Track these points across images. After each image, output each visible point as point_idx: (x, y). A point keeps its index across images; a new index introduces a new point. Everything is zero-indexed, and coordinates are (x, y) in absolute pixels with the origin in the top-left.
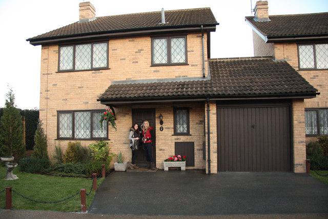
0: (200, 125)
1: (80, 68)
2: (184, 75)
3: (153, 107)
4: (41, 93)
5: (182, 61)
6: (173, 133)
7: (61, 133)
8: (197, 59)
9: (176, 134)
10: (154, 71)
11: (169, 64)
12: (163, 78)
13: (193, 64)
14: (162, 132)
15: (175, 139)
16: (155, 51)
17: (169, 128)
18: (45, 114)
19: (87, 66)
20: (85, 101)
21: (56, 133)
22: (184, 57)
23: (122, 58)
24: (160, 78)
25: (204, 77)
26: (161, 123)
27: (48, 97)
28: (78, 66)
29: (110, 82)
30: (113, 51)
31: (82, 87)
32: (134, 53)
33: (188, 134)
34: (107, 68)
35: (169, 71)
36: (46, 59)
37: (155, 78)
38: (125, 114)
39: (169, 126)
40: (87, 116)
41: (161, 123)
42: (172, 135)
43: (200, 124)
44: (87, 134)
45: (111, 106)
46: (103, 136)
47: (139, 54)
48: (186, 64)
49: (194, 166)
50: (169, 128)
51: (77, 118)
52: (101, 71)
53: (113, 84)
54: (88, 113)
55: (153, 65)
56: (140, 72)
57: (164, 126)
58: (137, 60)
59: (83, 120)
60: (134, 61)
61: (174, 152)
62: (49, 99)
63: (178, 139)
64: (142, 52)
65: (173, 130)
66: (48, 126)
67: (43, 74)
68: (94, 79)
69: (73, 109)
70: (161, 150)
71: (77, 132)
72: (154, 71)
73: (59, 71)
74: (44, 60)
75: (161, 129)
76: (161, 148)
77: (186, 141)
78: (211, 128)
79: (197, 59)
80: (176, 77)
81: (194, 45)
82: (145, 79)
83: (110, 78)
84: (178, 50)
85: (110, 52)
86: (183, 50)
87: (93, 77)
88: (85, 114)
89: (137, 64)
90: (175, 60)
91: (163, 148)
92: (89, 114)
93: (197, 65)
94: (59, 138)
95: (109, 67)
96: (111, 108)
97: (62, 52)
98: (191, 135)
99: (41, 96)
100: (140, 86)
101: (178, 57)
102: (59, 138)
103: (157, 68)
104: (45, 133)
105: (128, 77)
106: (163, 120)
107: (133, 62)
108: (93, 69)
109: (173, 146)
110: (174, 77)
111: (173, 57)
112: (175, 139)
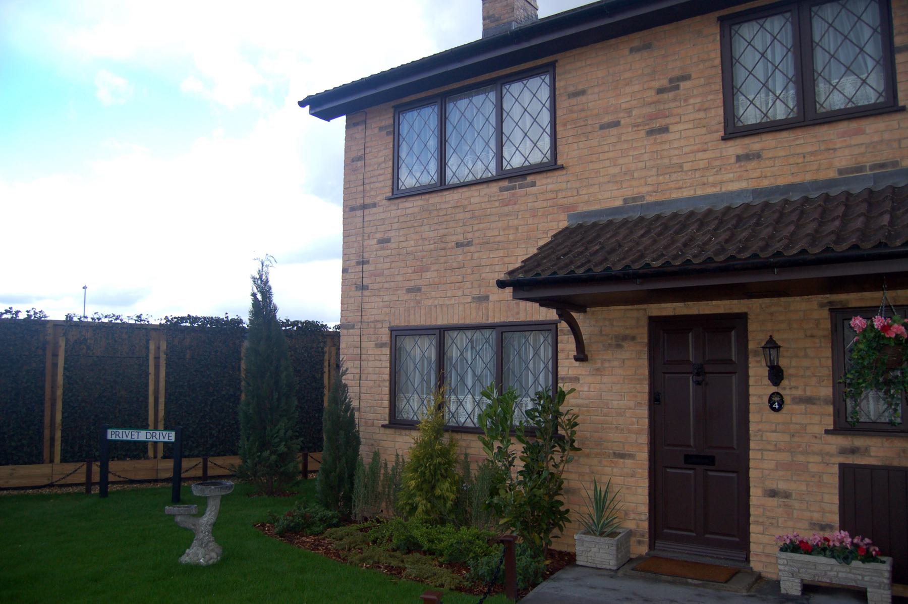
1: (464, 175)
4: (345, 271)
6: (829, 422)
10: (739, 158)
12: (781, 182)
15: (843, 451)
16: (741, 75)
17: (809, 401)
18: (357, 339)
20: (476, 292)
21: (386, 403)
23: (607, 119)
24: (765, 183)
27: (366, 282)
28: (457, 170)
30: (574, 101)
31: (469, 243)
32: (653, 93)
34: (551, 166)
36: (359, 159)
37: (743, 185)
38: (620, 341)
41: (776, 375)
42: (827, 432)
47: (671, 95)
50: (809, 401)
52: (530, 179)
57: (787, 389)
61: (836, 508)
62: (367, 288)
63: (853, 451)
64: (683, 85)
65: (830, 409)
66: (364, 382)
67: (353, 209)
69: (441, 321)
70: (773, 494)
73: (398, 194)
74: (355, 161)
75: (776, 403)
76: (772, 485)
77: (896, 463)
80: (841, 171)
82: (699, 192)
83: (561, 201)
85: (563, 104)
86: (872, 48)
87: (505, 203)
89: (665, 137)
91: (782, 486)
94: (396, 423)
96: (564, 315)
97: (404, 128)
99: (344, 279)
101: (840, 90)
103: (754, 144)
104: (355, 404)
105: (629, 193)
106: (783, 363)
107: (651, 132)
111: (822, 87)
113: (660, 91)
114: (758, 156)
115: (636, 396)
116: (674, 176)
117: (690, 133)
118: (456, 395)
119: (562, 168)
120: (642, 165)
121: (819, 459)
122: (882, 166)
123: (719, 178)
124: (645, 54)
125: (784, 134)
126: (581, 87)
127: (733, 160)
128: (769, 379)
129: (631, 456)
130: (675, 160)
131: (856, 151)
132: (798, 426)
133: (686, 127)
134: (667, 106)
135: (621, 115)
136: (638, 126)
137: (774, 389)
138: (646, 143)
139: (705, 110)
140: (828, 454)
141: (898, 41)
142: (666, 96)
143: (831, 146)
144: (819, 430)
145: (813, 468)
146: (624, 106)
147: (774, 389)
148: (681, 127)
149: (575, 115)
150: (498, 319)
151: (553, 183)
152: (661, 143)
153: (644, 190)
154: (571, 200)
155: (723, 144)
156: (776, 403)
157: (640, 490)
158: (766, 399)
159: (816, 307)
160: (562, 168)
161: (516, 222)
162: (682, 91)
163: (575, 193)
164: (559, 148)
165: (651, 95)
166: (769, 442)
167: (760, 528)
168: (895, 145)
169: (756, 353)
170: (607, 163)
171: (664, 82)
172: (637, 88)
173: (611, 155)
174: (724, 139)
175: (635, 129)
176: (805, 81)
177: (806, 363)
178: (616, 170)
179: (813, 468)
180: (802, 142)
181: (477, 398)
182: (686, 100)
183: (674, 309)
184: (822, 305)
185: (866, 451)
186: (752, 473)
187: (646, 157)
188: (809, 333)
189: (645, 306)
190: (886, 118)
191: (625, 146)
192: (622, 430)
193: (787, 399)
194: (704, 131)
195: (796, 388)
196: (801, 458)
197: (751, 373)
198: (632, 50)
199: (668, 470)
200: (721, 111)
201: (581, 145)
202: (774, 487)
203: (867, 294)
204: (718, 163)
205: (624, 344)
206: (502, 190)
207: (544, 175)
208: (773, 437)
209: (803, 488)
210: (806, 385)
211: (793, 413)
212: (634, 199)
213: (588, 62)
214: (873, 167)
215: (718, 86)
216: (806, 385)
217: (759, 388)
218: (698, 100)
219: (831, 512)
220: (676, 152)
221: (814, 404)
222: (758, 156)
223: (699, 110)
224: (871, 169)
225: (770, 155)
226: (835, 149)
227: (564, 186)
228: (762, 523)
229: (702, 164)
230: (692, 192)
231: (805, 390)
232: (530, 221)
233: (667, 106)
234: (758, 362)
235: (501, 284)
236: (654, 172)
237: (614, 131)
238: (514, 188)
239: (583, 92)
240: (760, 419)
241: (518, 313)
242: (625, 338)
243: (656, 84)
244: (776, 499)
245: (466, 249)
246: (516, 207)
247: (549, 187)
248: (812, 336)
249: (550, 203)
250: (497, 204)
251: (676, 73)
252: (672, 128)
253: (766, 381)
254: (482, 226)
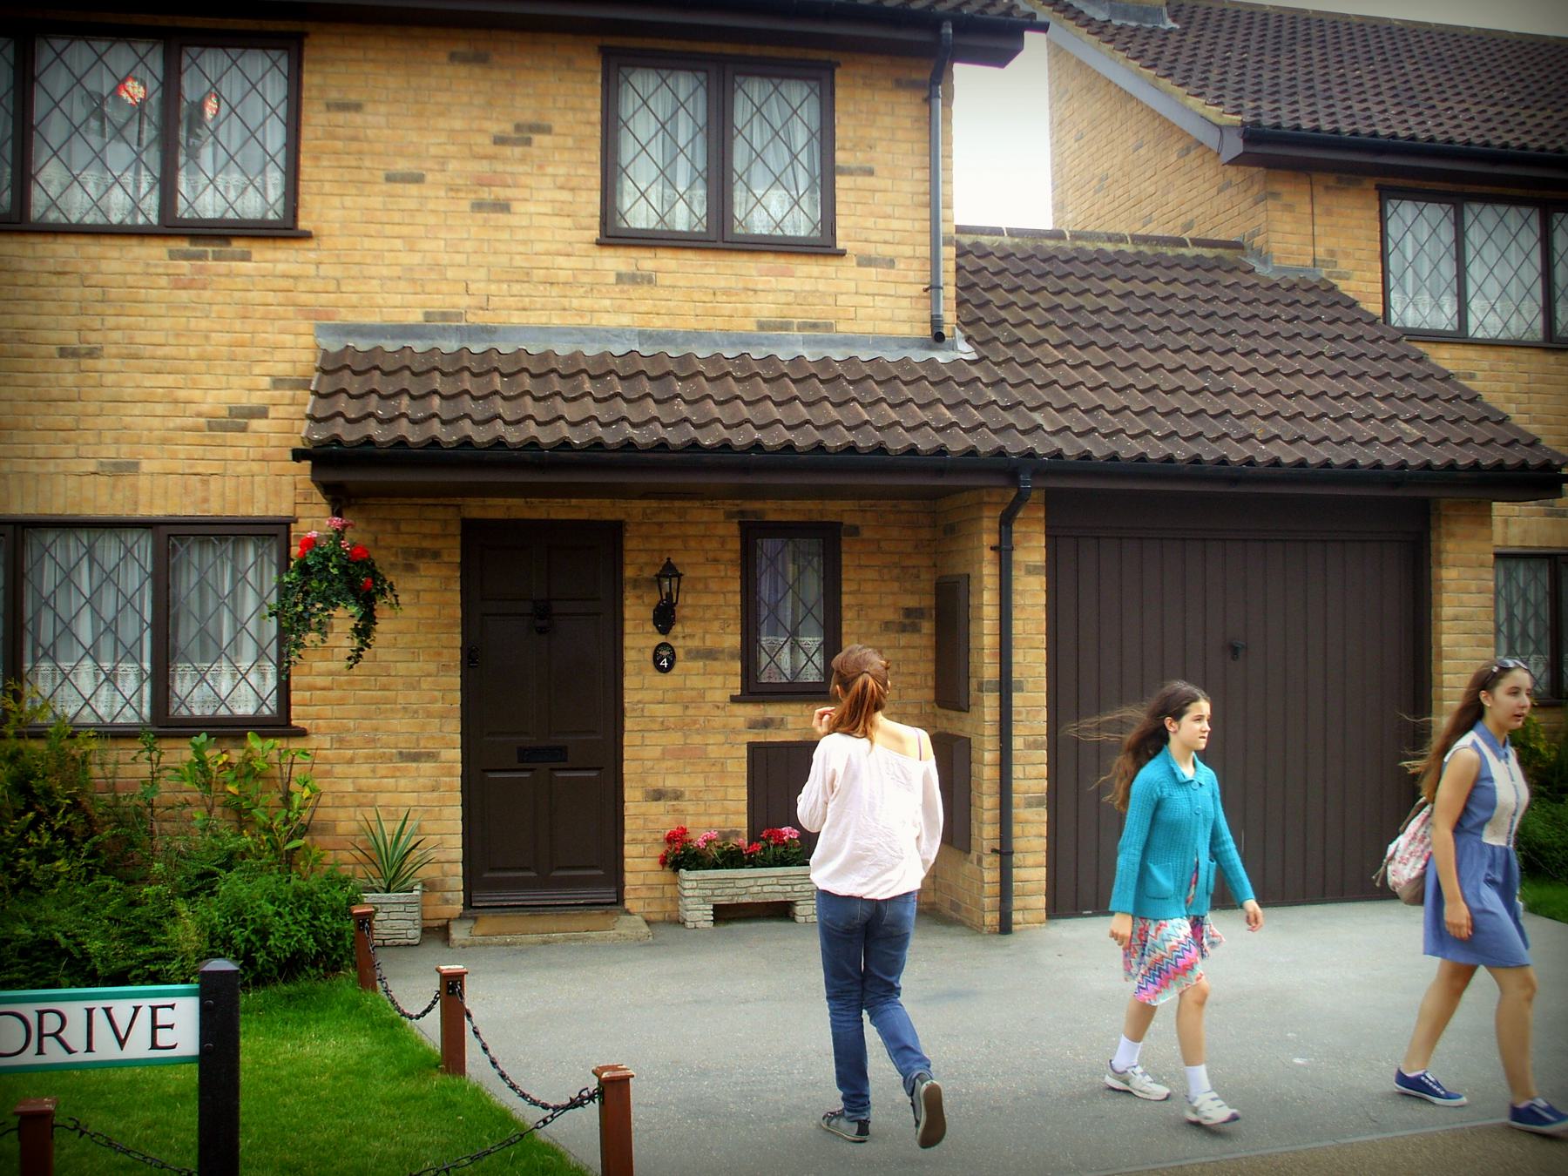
0: (904, 639)
2: (815, 313)
5: (801, 226)
8: (895, 224)
9: (754, 690)
10: (620, 278)
11: (720, 236)
12: (680, 325)
13: (871, 250)
14: (660, 679)
15: (753, 725)
16: (628, 149)
23: (402, 165)
24: (658, 323)
25: (939, 337)
26: (665, 618)
29: (304, 326)
30: (340, 118)
32: (487, 141)
34: (284, 229)
35: (722, 283)
37: (625, 320)
38: (412, 559)
39: (709, 642)
41: (665, 618)
42: (734, 700)
43: (903, 629)
46: (245, 707)
50: (710, 654)
52: (238, 246)
55: (613, 236)
56: (525, 277)
57: (683, 638)
58: (501, 193)
60: (486, 194)
61: (743, 806)
63: (767, 724)
64: (538, 139)
68: (184, 295)
70: (658, 795)
72: (620, 278)
75: (664, 660)
76: (657, 782)
78: (1018, 657)
79: (895, 224)
80: (762, 326)
81: (875, 133)
82: (556, 321)
84: (777, 157)
87: (179, 283)
89: (502, 218)
91: (670, 782)
92: (143, 546)
93: (890, 263)
95: (303, 224)
100: (550, 374)
103: (647, 261)
105: (438, 303)
107: (479, 206)
108: (170, 226)
109: (739, 767)
110: (750, 326)
112: (753, 725)
113: (500, 140)
114: (649, 280)
115: (439, 654)
116: (516, 288)
117: (545, 221)
118: (54, 659)
119: (307, 236)
120: (460, 258)
121: (721, 738)
122: (814, 326)
123: (587, 303)
124: (477, 71)
125: (689, 255)
126: (353, 97)
127: (612, 279)
128: (655, 624)
129: (431, 756)
130: (518, 261)
131: (783, 298)
132: (694, 693)
133: (543, 209)
134: (509, 168)
135: (429, 164)
136: (458, 191)
137: (661, 639)
138: (469, 221)
139: (572, 189)
140: (734, 731)
141: (841, 157)
142: (507, 151)
143: (750, 286)
144: (721, 696)
145: (714, 752)
146: (433, 151)
147: (661, 639)
148: (531, 208)
149: (339, 145)
150: (158, 511)
151: (287, 261)
152: (497, 228)
153: (463, 302)
154: (324, 299)
155: (597, 252)
156: (664, 660)
157: (447, 812)
158: (649, 655)
159: (722, 518)
160: (307, 236)
161: (204, 324)
162: (534, 150)
163: (332, 287)
164: (304, 198)
165: (484, 143)
166: (653, 718)
167: (640, 849)
168: (830, 300)
169: (636, 583)
170: (398, 244)
171: (507, 128)
172: (458, 124)
173: (405, 230)
174: (599, 243)
175: (452, 194)
176: (719, 181)
177: (706, 600)
178: (416, 259)
179: (714, 752)
180: (713, 270)
181: (107, 665)
182: (541, 167)
183: (508, 508)
184: (729, 515)
185: (779, 724)
186: (628, 767)
187: (469, 246)
188: (711, 555)
189: (458, 501)
190: (821, 260)
191: (432, 220)
192: (416, 712)
193: (680, 653)
194: (568, 222)
195: (692, 636)
196: (696, 739)
197: (628, 614)
198: (453, 57)
199: (491, 775)
200: (596, 197)
201: (348, 201)
202: (660, 785)
203: (789, 504)
204: (585, 279)
205: (422, 565)
206: (173, 256)
207: (270, 243)
208: (659, 710)
209: (700, 782)
210: (706, 632)
211: (688, 673)
212: (445, 316)
213: (371, 55)
214: (802, 327)
215: (596, 156)
216: (706, 632)
217: (639, 640)
218: (562, 170)
219: (737, 813)
220: (521, 249)
221: (715, 659)
222: (649, 280)
223: (561, 188)
224: (799, 329)
225: (667, 283)
226: (755, 291)
227: (311, 270)
228: (642, 842)
229: (563, 276)
230: (544, 320)
231: (703, 639)
232: (238, 325)
233: (509, 168)
234: (640, 597)
235: (298, 455)
236: (482, 273)
237: (413, 189)
238: (201, 256)
239: (357, 107)
240: (641, 688)
241: (206, 500)
242: (421, 554)
243: (495, 128)
244: (661, 803)
245: (88, 363)
246: (207, 295)
247: (281, 268)
248: (716, 560)
249: (281, 297)
250: (163, 281)
251: (528, 117)
252: (516, 207)
253: (650, 627)
254: (124, 321)
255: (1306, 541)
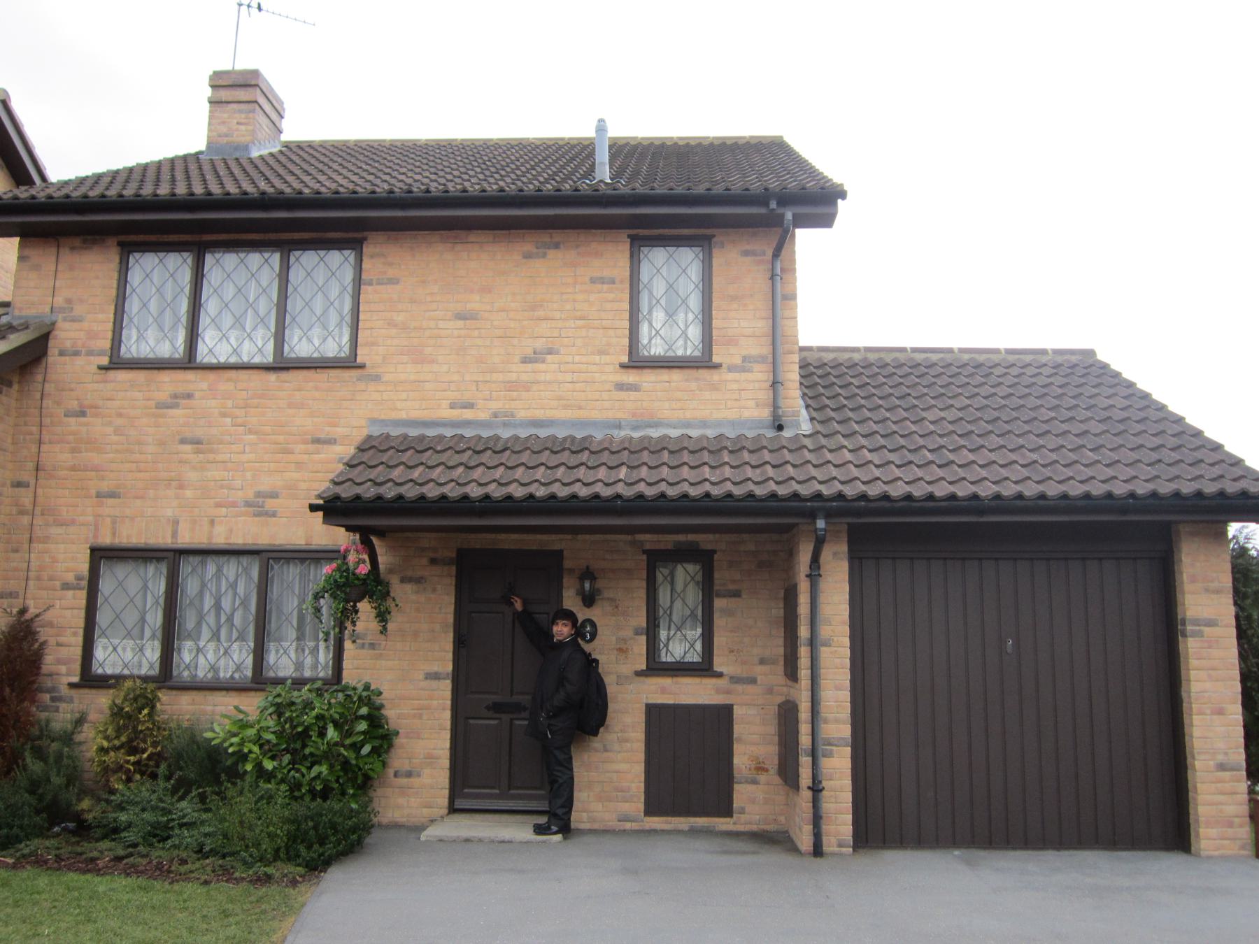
3: (555, 542)
7: (99, 653)
19: (258, 347)
22: (695, 332)
33: (704, 668)
40: (238, 582)
44: (236, 659)
45: (365, 536)
48: (703, 362)
49: (727, 811)
51: (190, 585)
53: (376, 431)
54: (245, 560)
59: (223, 593)
71: (186, 653)
88: (231, 568)
90: (658, 341)
98: (720, 675)
102: (90, 680)
255: (964, 559)
